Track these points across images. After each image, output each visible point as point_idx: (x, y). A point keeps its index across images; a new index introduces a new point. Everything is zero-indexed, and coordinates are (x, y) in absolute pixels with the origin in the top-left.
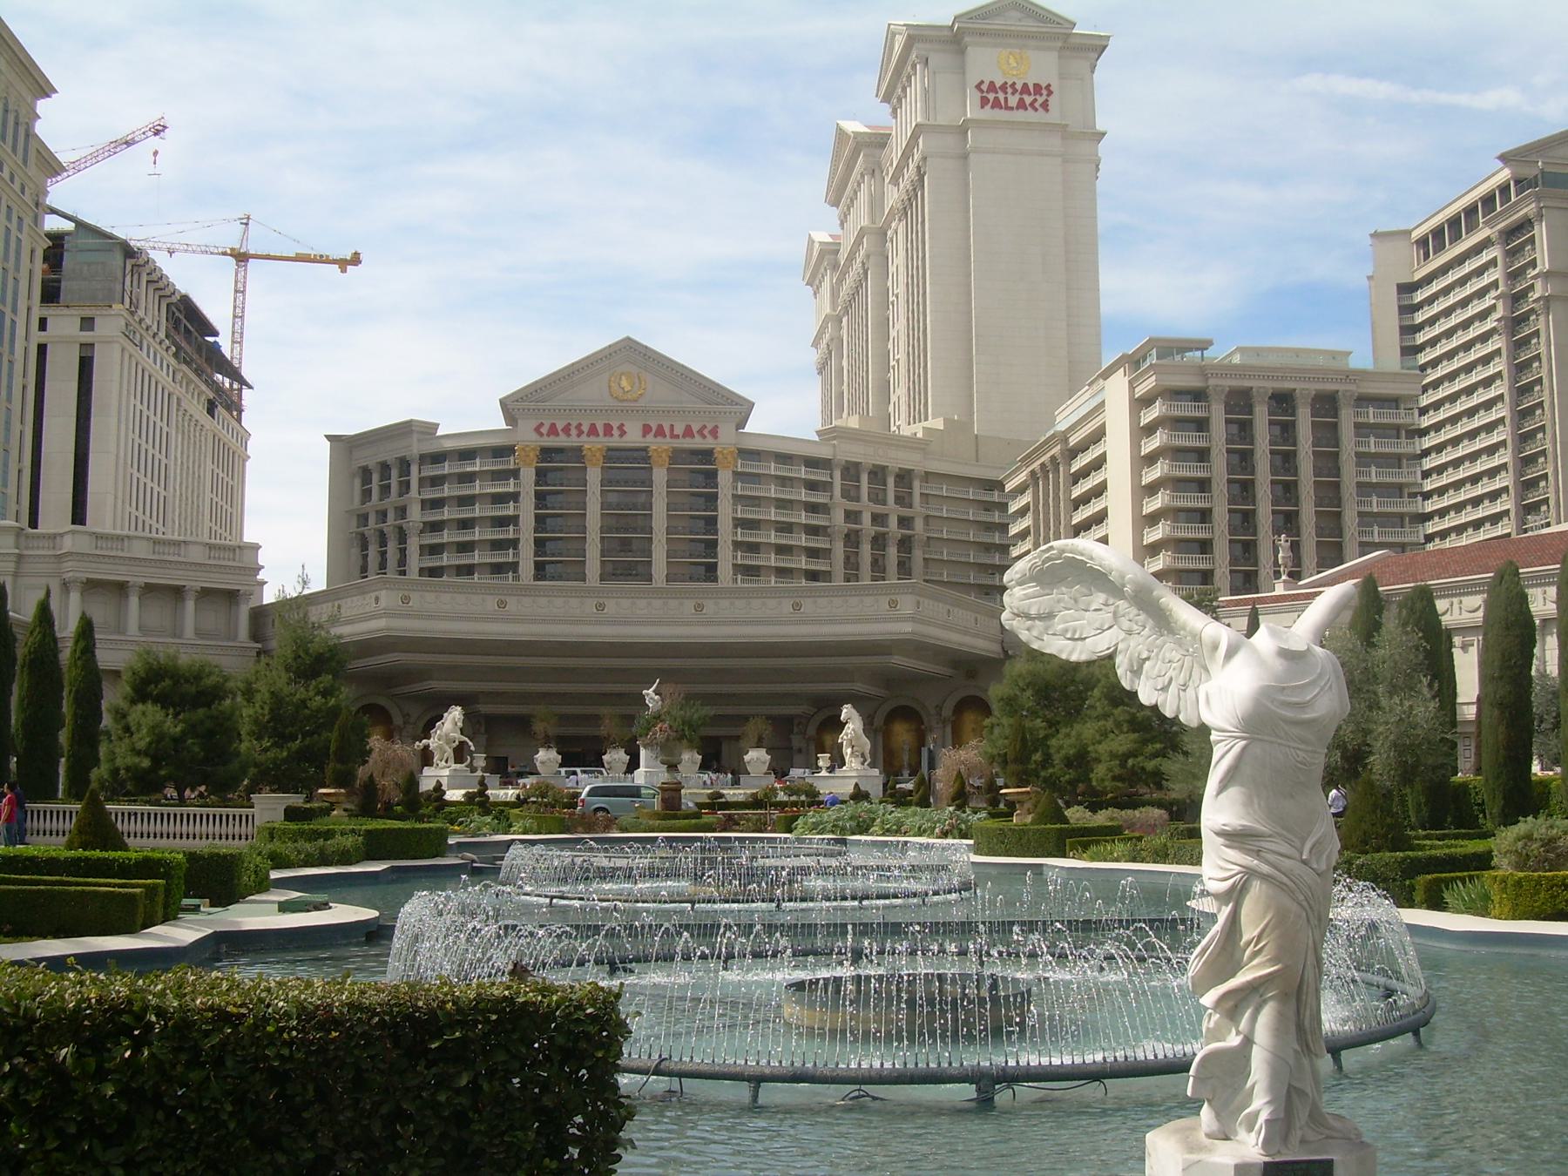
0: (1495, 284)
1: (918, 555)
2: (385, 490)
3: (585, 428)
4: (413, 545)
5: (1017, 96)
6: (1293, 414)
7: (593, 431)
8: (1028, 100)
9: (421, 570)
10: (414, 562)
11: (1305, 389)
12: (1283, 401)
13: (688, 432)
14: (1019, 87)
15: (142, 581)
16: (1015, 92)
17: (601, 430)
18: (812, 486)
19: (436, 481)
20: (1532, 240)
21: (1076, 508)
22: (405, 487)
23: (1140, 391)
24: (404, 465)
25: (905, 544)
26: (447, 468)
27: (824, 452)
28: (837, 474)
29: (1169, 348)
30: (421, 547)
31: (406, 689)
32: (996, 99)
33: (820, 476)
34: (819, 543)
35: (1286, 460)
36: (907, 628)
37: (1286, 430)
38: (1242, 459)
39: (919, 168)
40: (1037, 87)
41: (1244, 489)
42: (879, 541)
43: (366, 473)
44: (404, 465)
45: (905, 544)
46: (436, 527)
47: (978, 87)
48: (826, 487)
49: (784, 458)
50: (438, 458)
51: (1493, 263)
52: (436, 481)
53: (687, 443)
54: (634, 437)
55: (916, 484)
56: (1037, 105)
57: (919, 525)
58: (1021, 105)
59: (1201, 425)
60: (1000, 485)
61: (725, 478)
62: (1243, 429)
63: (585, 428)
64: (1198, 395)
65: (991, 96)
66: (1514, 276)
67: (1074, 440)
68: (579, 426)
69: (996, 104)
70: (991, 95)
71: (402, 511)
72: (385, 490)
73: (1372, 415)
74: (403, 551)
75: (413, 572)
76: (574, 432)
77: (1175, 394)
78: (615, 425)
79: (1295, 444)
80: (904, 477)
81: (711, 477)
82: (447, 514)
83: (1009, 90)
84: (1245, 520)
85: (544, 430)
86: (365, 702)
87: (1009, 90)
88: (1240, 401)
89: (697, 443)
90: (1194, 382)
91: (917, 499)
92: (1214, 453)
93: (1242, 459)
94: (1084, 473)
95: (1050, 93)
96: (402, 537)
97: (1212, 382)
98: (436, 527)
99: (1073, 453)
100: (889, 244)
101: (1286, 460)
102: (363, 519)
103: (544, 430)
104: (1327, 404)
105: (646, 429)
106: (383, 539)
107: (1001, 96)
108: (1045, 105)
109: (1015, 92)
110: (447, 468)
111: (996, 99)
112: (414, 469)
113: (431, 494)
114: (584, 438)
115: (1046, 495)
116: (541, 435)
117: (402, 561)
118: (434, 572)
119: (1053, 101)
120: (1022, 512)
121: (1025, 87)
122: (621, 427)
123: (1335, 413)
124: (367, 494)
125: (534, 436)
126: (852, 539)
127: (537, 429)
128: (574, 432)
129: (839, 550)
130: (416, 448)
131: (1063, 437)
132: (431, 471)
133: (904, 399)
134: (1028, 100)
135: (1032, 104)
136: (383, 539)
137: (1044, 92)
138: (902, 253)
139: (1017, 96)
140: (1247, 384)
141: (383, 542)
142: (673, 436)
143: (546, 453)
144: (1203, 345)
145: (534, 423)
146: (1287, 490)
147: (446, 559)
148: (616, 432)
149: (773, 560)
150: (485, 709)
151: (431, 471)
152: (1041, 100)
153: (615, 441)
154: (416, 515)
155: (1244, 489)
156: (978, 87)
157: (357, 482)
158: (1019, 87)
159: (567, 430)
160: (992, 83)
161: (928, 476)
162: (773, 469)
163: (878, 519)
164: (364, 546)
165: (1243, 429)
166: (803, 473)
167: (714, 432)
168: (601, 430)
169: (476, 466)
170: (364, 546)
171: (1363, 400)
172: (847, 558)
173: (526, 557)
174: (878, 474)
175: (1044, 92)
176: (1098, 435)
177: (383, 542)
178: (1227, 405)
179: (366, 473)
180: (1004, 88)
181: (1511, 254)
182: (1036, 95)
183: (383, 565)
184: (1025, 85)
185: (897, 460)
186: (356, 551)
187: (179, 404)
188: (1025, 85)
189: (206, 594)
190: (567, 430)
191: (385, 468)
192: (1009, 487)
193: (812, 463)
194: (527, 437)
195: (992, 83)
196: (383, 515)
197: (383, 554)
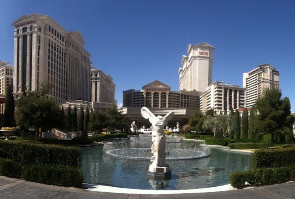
0: (257, 79)
1: (189, 105)
2: (129, 97)
4: (132, 103)
18: (177, 97)
19: (135, 96)
20: (261, 75)
22: (131, 97)
24: (131, 94)
25: (188, 104)
26: (136, 94)
33: (178, 96)
34: (178, 103)
42: (185, 103)
43: (127, 95)
44: (131, 94)
45: (188, 104)
46: (135, 101)
48: (179, 97)
49: (175, 94)
50: (135, 93)
51: (257, 77)
57: (190, 101)
60: (199, 97)
61: (167, 96)
66: (259, 78)
67: (207, 92)
71: (131, 99)
72: (129, 97)
80: (188, 96)
82: (136, 100)
91: (190, 98)
96: (131, 102)
98: (135, 101)
99: (207, 94)
106: (129, 102)
110: (136, 94)
126: (182, 103)
130: (133, 92)
131: (206, 92)
132: (134, 95)
136: (129, 102)
149: (173, 105)
153: (155, 91)
154: (133, 100)
161: (191, 96)
162: (173, 95)
164: (127, 103)
166: (176, 95)
170: (127, 103)
174: (185, 96)
179: (127, 95)
181: (259, 76)
185: (187, 94)
191: (129, 94)
192: (200, 97)
193: (178, 94)
196: (129, 100)
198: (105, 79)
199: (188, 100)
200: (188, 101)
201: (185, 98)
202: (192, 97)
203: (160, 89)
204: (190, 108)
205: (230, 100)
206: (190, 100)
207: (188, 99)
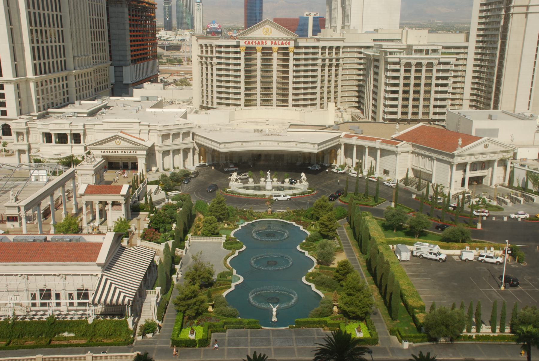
2: (207, 52)
3: (257, 42)
4: (215, 68)
13: (282, 44)
22: (212, 52)
28: (320, 50)
43: (201, 46)
53: (282, 46)
54: (269, 44)
61: (291, 54)
72: (207, 52)
76: (254, 43)
81: (288, 54)
85: (247, 43)
89: (285, 46)
102: (201, 57)
103: (247, 43)
105: (272, 43)
112: (214, 48)
124: (202, 51)
125: (244, 44)
127: (245, 43)
128: (254, 43)
129: (320, 69)
142: (279, 44)
145: (245, 41)
148: (264, 43)
153: (264, 45)
157: (200, 47)
159: (252, 43)
164: (202, 64)
167: (289, 43)
186: (200, 66)
197: (207, 68)
203: (274, 39)
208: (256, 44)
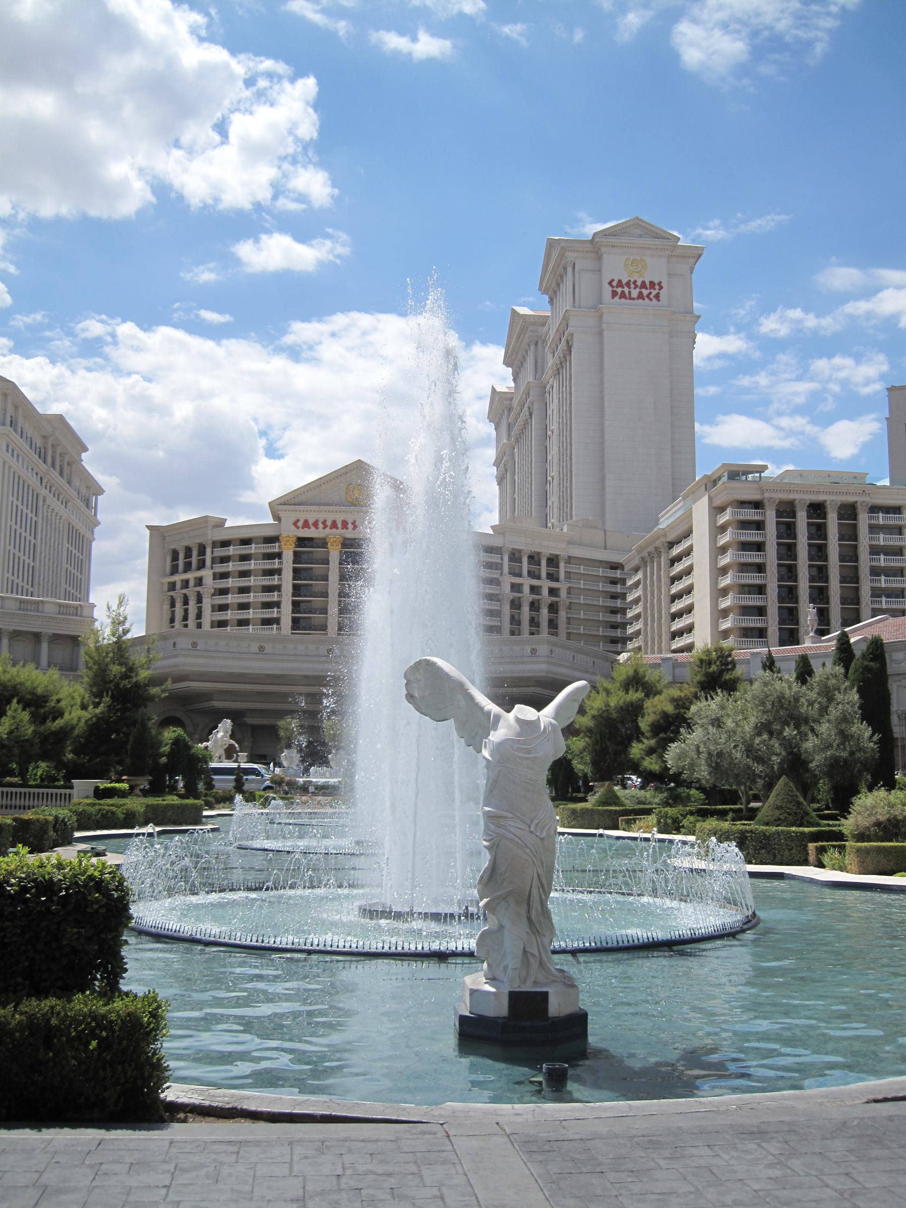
1: (563, 614)
3: (329, 523)
5: (638, 290)
6: (825, 518)
7: (334, 525)
8: (645, 292)
9: (212, 622)
10: (208, 616)
11: (833, 500)
12: (817, 509)
14: (639, 283)
15: (11, 628)
16: (636, 287)
17: (339, 525)
19: (225, 560)
21: (673, 583)
23: (717, 503)
25: (553, 608)
26: (231, 551)
27: (498, 542)
28: (506, 558)
29: (735, 474)
30: (213, 606)
31: (197, 706)
32: (623, 292)
35: (819, 552)
36: (544, 667)
37: (818, 531)
38: (788, 551)
39: (568, 342)
40: (652, 284)
41: (789, 572)
43: (175, 555)
44: (202, 549)
45: (553, 608)
46: (224, 592)
47: (610, 283)
50: (225, 544)
52: (225, 560)
55: (562, 565)
56: (652, 296)
57: (563, 593)
58: (640, 296)
59: (759, 525)
62: (787, 530)
63: (329, 523)
64: (757, 505)
65: (619, 290)
67: (670, 538)
68: (324, 522)
69: (623, 295)
70: (620, 289)
73: (881, 519)
74: (200, 610)
75: (206, 625)
76: (321, 526)
77: (743, 504)
78: (350, 521)
79: (826, 539)
80: (553, 561)
83: (632, 286)
84: (789, 594)
85: (300, 524)
86: (167, 715)
87: (632, 286)
88: (787, 510)
90: (755, 496)
91: (562, 576)
92: (768, 546)
93: (788, 551)
94: (679, 558)
95: (661, 288)
96: (199, 599)
97: (767, 495)
98: (224, 592)
99: (671, 545)
100: (547, 394)
101: (819, 552)
103: (300, 524)
104: (849, 512)
107: (626, 290)
108: (657, 297)
109: (636, 287)
111: (623, 292)
112: (208, 551)
113: (220, 568)
114: (328, 529)
115: (652, 574)
116: (298, 527)
117: (199, 616)
118: (222, 624)
119: (663, 293)
120: (636, 585)
121: (643, 285)
122: (354, 523)
123: (854, 517)
124: (174, 570)
127: (295, 524)
128: (321, 526)
132: (220, 552)
133: (556, 504)
134: (645, 292)
135: (648, 296)
137: (657, 287)
138: (556, 401)
139: (638, 290)
140: (792, 496)
141: (186, 601)
143: (301, 541)
144: (762, 469)
146: (820, 573)
147: (229, 615)
148: (350, 526)
150: (250, 721)
151: (220, 552)
152: (654, 292)
155: (789, 572)
156: (610, 283)
157: (169, 559)
158: (639, 283)
159: (316, 524)
160: (620, 281)
161: (569, 560)
163: (534, 589)
164: (173, 605)
165: (787, 530)
168: (339, 525)
169: (253, 549)
170: (173, 605)
171: (874, 509)
172: (512, 617)
173: (286, 613)
174: (534, 559)
175: (657, 287)
176: (688, 533)
177: (186, 601)
178: (777, 511)
180: (628, 284)
182: (650, 290)
183: (185, 618)
184: (643, 282)
186: (166, 607)
187: (44, 500)
188: (643, 282)
189: (56, 638)
190: (316, 524)
194: (289, 532)
195: (620, 281)
198: (39, 442)
199: (554, 585)
200: (553, 592)
201: (532, 575)
202: (573, 569)
204: (569, 635)
205: (820, 573)
206: (562, 586)
207: (552, 577)
208: (325, 527)
